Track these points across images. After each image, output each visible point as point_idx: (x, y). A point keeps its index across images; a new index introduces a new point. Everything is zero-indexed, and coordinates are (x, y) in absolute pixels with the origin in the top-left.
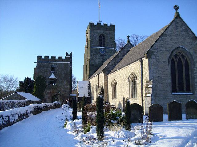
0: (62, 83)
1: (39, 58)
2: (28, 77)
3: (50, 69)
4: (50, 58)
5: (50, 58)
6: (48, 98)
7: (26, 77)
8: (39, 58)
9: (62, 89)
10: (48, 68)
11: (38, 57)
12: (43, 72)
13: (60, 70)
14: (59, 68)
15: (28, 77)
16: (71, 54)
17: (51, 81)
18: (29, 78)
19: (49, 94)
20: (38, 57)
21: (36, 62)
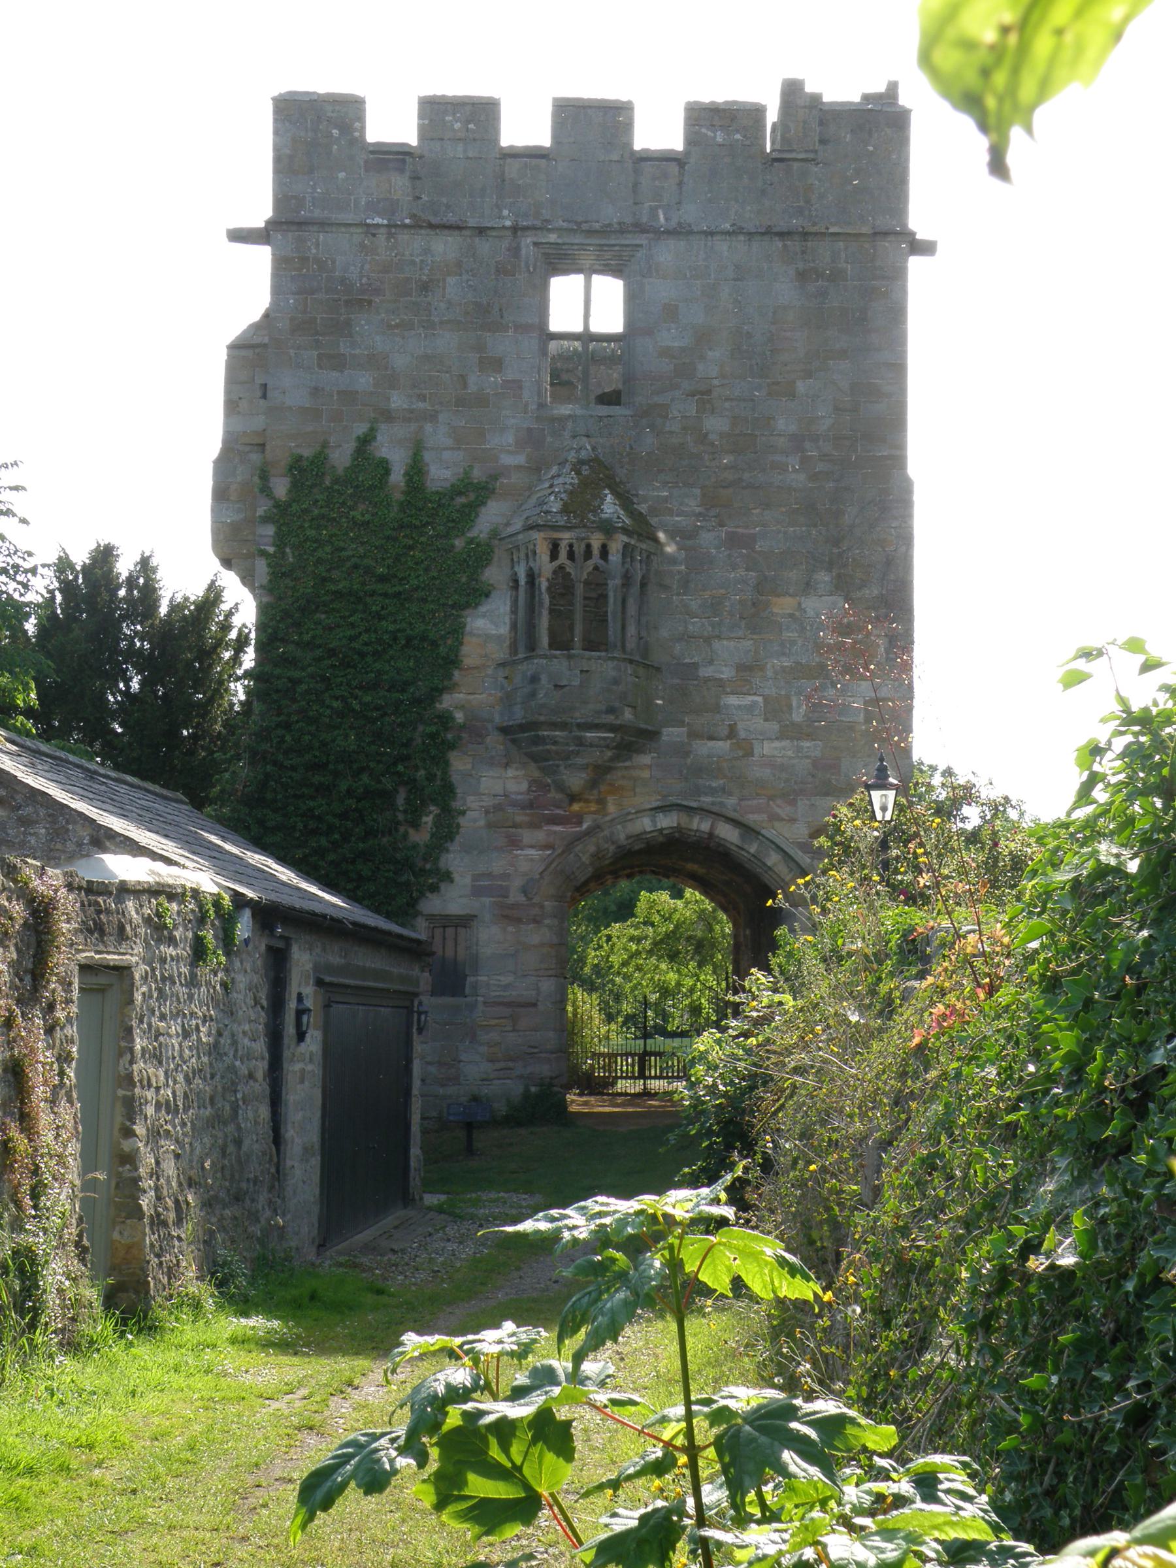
0: (755, 617)
1: (314, 130)
2: (105, 556)
4: (525, 127)
6: (509, 915)
7: (80, 557)
8: (314, 130)
9: (768, 748)
15: (105, 556)
17: (562, 585)
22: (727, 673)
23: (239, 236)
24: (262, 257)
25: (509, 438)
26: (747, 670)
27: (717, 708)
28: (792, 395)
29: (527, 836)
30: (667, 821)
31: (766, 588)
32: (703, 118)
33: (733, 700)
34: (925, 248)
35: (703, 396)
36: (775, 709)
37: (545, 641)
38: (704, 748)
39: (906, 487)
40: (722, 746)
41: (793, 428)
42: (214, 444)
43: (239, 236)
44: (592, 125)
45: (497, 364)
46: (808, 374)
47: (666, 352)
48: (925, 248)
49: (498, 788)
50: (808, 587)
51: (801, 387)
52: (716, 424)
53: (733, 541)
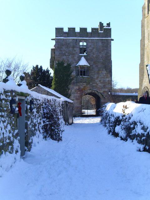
0: (98, 73)
1: (59, 31)
2: (37, 66)
3: (78, 50)
4: (77, 30)
5: (77, 30)
7: (35, 66)
8: (59, 31)
9: (99, 84)
10: (75, 49)
11: (57, 29)
12: (66, 55)
13: (94, 50)
14: (93, 48)
15: (37, 66)
16: (109, 25)
17: (81, 71)
18: (39, 67)
19: (77, 93)
20: (57, 29)
21: (54, 37)
22: (96, 78)
23: (52, 39)
24: (54, 41)
25: (76, 57)
26: (98, 78)
27: (95, 81)
28: (101, 53)
29: (78, 92)
30: (91, 91)
31: (99, 70)
32: (92, 29)
33: (96, 80)
34: (113, 40)
35: (93, 54)
36: (100, 81)
37: (80, 74)
38: (94, 84)
39: (111, 61)
40: (95, 84)
41: (101, 56)
42: (50, 57)
43: (52, 39)
44: (83, 30)
45: (75, 51)
46: (103, 51)
47: (90, 49)
48: (113, 40)
49: (76, 88)
50: (103, 70)
51: (102, 52)
52: (94, 56)
53: (96, 66)
